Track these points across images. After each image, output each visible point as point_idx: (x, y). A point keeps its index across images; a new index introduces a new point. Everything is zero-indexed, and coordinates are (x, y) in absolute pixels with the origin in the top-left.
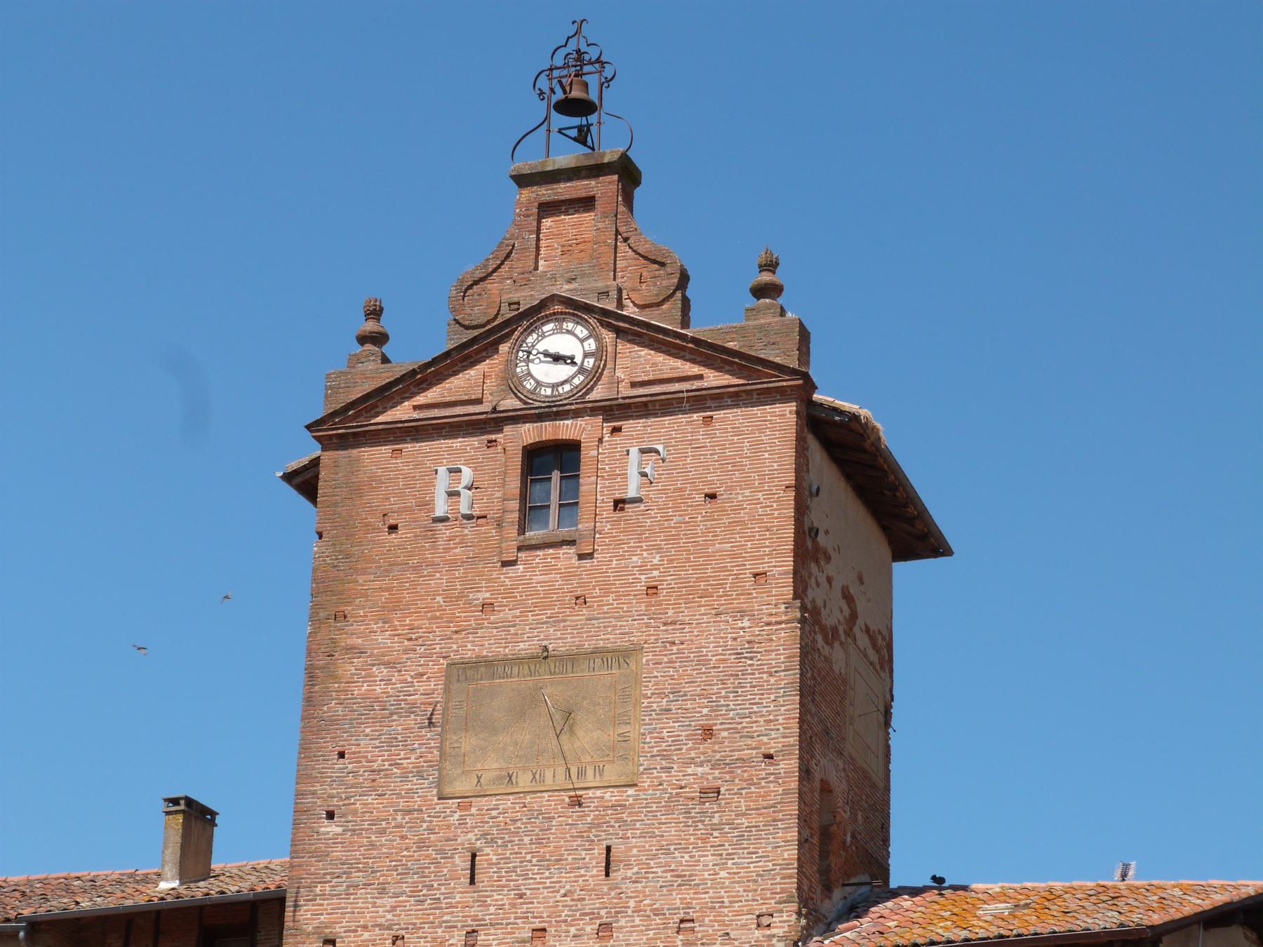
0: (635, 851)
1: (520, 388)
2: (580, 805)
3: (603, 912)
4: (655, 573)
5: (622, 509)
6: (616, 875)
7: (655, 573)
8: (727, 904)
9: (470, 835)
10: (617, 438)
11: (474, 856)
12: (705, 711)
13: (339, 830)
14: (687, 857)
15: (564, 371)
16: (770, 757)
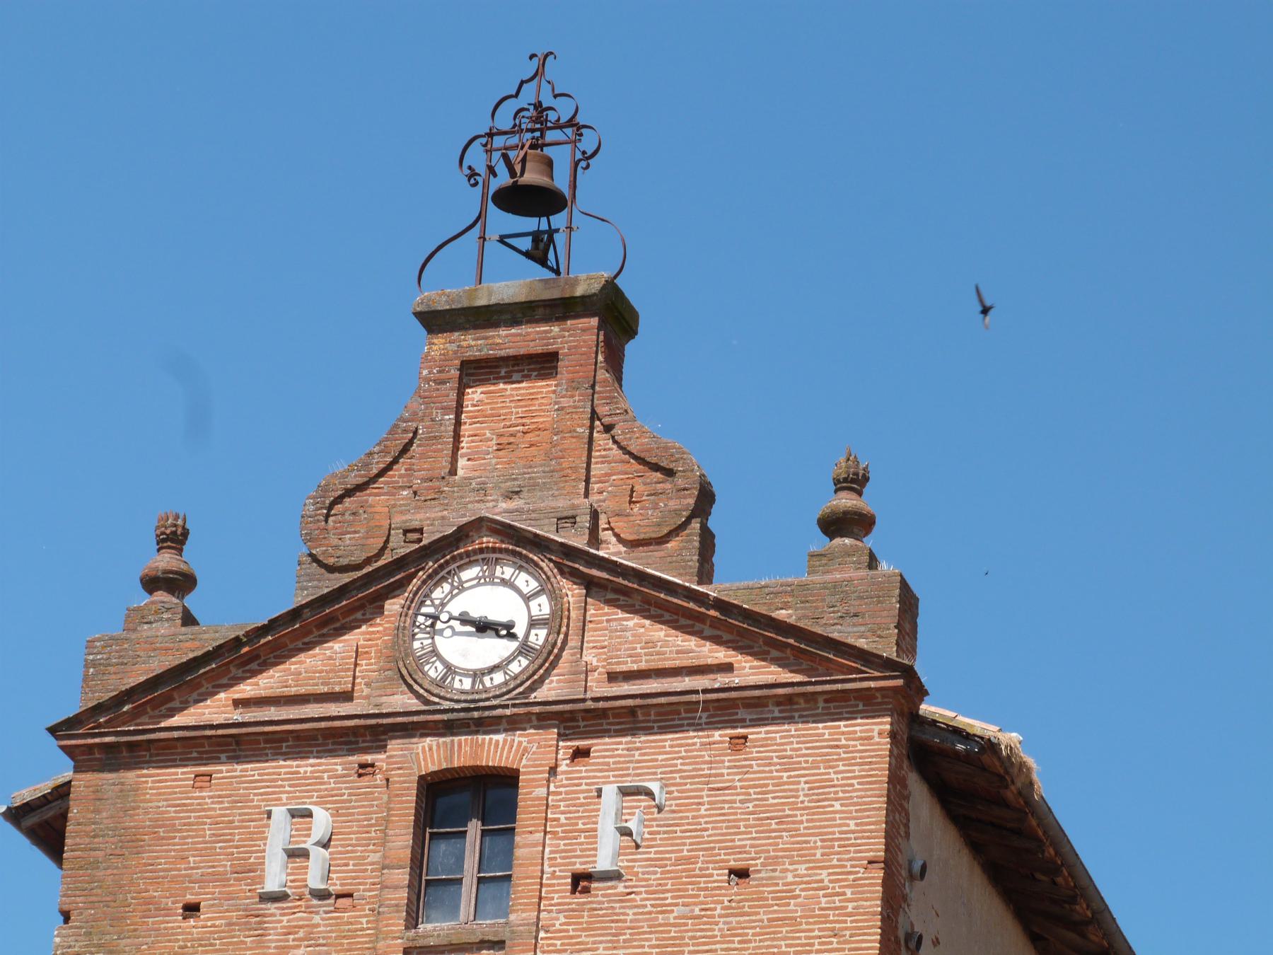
1: (418, 676)
5: (586, 891)
10: (582, 768)
15: (494, 649)
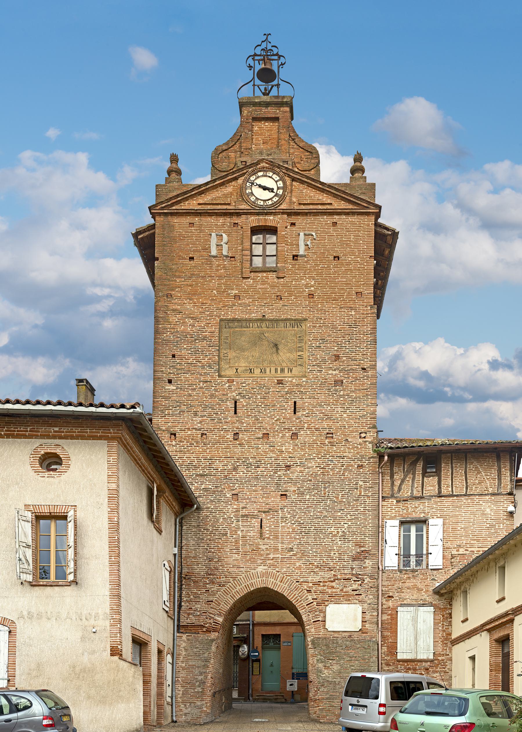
0: (307, 404)
1: (249, 200)
2: (282, 384)
3: (293, 428)
4: (312, 289)
5: (297, 260)
6: (299, 414)
7: (312, 289)
8: (347, 428)
9: (234, 393)
10: (294, 228)
11: (236, 402)
12: (336, 348)
13: (175, 388)
14: (329, 408)
15: (267, 195)
16: (364, 369)
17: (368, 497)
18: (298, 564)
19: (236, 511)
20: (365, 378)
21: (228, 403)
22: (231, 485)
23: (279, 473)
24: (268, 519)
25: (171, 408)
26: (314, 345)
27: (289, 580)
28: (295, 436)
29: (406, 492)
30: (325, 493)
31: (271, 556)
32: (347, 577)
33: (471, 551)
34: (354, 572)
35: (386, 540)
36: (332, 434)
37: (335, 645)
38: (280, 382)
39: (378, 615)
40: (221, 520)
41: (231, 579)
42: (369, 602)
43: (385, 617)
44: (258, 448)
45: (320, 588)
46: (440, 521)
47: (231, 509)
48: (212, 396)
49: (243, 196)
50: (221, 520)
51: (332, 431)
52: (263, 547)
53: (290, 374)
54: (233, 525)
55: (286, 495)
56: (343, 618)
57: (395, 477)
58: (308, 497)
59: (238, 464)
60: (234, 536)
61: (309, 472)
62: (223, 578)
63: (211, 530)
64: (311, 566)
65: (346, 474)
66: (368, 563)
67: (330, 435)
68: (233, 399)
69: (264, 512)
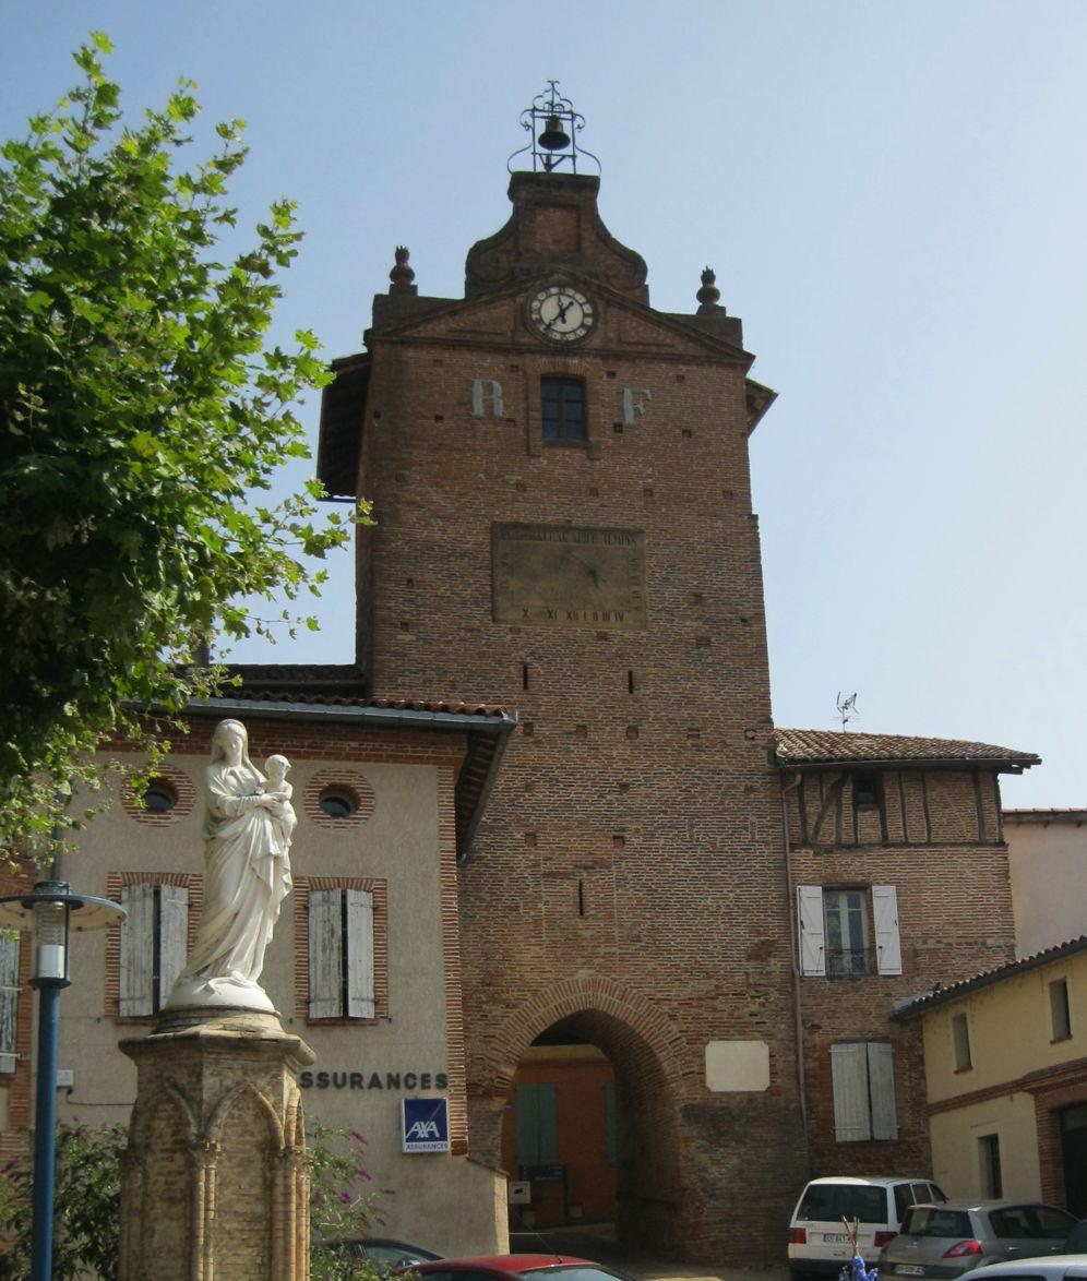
0: (651, 677)
2: (606, 640)
3: (630, 718)
4: (650, 480)
6: (639, 692)
7: (650, 480)
8: (722, 719)
9: (521, 653)
11: (525, 669)
12: (695, 583)
13: (414, 638)
14: (690, 685)
16: (744, 620)
17: (767, 844)
18: (650, 966)
19: (534, 866)
20: (748, 635)
21: (512, 668)
22: (523, 816)
23: (608, 797)
24: (593, 882)
25: (407, 673)
26: (657, 575)
27: (637, 996)
28: (632, 731)
29: (828, 835)
30: (691, 836)
31: (601, 950)
32: (739, 990)
33: (946, 944)
34: (751, 981)
35: (802, 923)
36: (698, 731)
37: (723, 1118)
38: (602, 637)
39: (797, 1061)
40: (507, 881)
41: (529, 994)
42: (779, 1036)
43: (811, 1064)
44: (568, 751)
45: (694, 1011)
46: (891, 890)
47: (522, 861)
48: (482, 655)
49: (524, 319)
50: (507, 881)
51: (697, 725)
52: (587, 934)
53: (618, 624)
54: (528, 892)
55: (622, 837)
56: (737, 1066)
57: (808, 808)
58: (662, 842)
59: (533, 779)
60: (532, 913)
61: (663, 796)
62: (513, 991)
63: (488, 899)
64: (673, 970)
65: (727, 802)
66: (775, 964)
67: (694, 733)
68: (521, 663)
69: (586, 868)
